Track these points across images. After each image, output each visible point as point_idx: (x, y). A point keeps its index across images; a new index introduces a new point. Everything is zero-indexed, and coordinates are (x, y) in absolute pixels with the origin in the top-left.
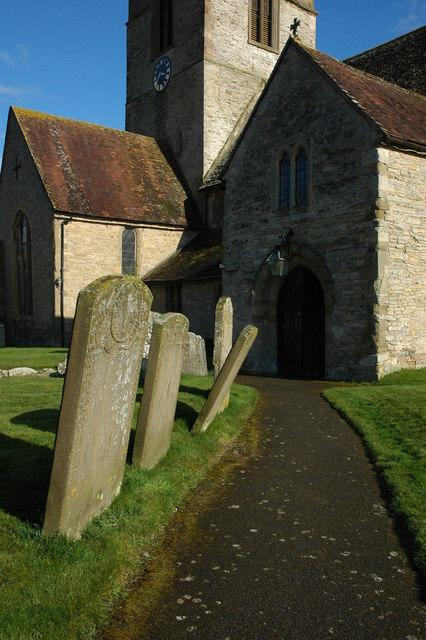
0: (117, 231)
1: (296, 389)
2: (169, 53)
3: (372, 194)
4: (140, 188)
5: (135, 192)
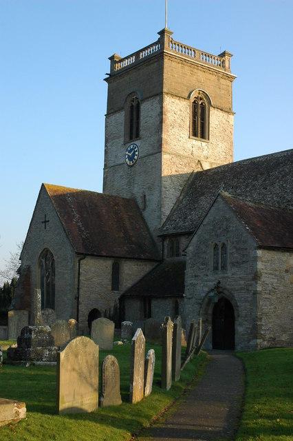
0: (109, 263)
2: (138, 143)
4: (122, 235)
5: (119, 237)
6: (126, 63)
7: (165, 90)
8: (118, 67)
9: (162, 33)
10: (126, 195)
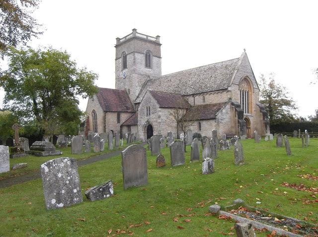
2: (126, 70)
9: (134, 30)
10: (123, 89)
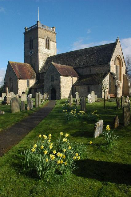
0: (26, 80)
1: (53, 101)
3: (60, 81)
6: (29, 30)
7: (39, 37)
8: (27, 30)
